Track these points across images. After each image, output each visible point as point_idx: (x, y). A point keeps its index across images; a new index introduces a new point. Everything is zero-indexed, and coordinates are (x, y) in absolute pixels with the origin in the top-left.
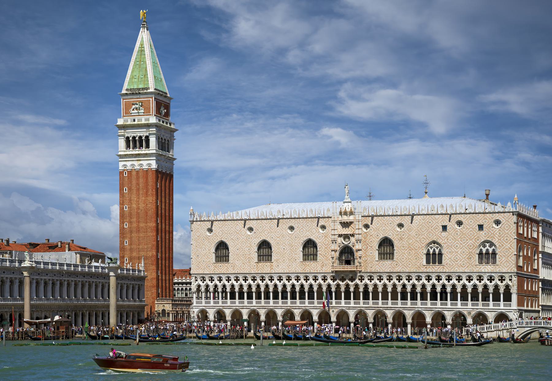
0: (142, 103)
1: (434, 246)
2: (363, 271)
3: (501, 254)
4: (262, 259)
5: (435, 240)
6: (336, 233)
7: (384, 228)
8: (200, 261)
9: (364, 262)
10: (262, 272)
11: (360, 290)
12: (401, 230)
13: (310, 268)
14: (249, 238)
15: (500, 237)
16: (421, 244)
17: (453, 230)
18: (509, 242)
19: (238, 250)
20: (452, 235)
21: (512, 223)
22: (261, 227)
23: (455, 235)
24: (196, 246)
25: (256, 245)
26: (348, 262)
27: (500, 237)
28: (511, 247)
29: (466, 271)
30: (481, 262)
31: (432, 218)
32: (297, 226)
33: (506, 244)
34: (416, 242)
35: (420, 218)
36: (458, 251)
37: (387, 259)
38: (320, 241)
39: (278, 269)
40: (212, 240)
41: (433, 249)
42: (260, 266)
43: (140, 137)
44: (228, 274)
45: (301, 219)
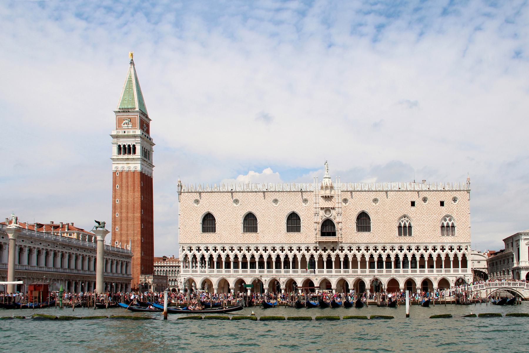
2: (344, 242)
5: (406, 214)
6: (317, 207)
9: (344, 234)
11: (341, 260)
12: (376, 205)
13: (294, 239)
14: (235, 210)
15: (457, 212)
16: (394, 217)
17: (420, 206)
18: (465, 216)
19: (224, 221)
22: (246, 199)
23: (422, 210)
26: (329, 234)
27: (457, 212)
38: (303, 214)
40: (199, 211)
41: (403, 222)
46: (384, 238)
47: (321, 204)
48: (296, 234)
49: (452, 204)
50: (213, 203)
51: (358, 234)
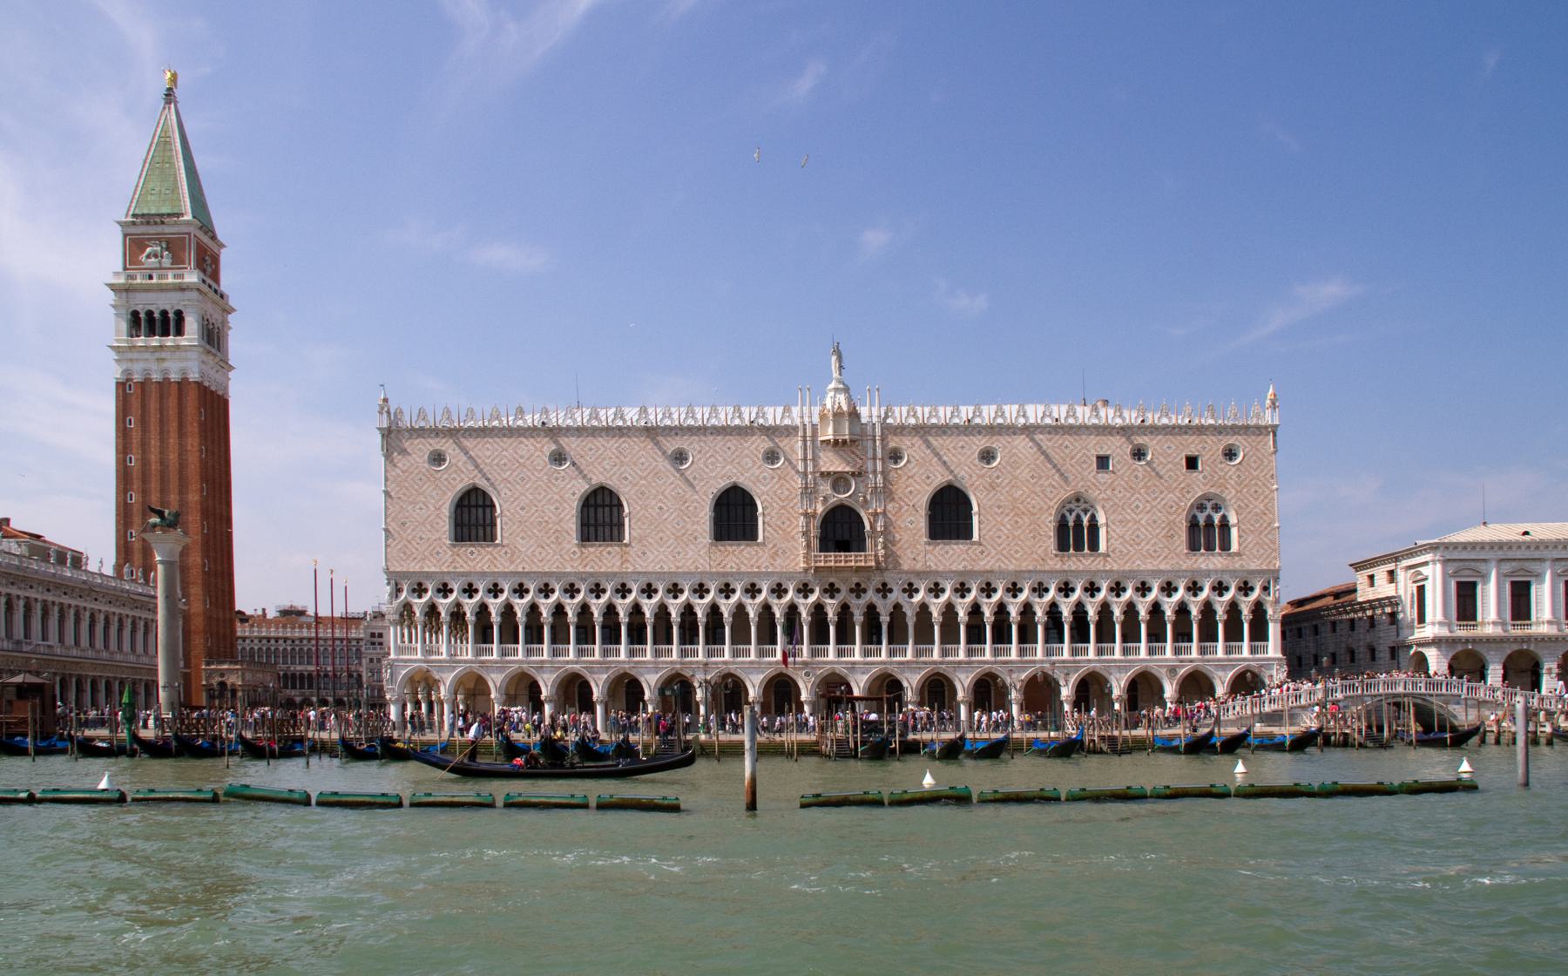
2: (891, 566)
3: (1243, 527)
4: (592, 535)
5: (1083, 490)
8: (409, 538)
10: (597, 569)
14: (557, 479)
18: (1262, 497)
19: (523, 509)
22: (591, 449)
24: (399, 498)
25: (578, 496)
26: (844, 546)
28: (1267, 509)
32: (699, 449)
33: (1254, 502)
34: (1032, 495)
39: (644, 561)
41: (1074, 514)
42: (590, 553)
43: (164, 313)
50: (487, 461)
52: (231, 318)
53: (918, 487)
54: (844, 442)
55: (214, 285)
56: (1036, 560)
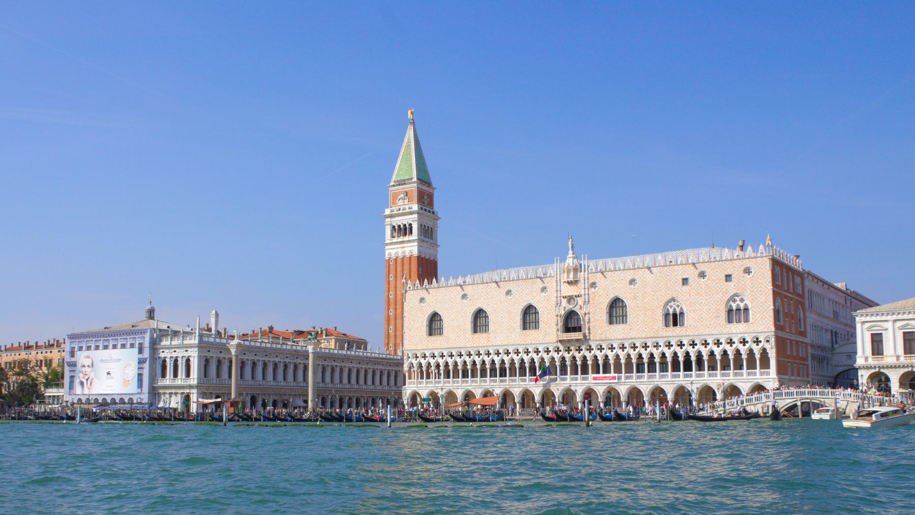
0: (407, 193)
1: (674, 304)
2: (592, 338)
3: (755, 310)
5: (675, 296)
7: (615, 286)
10: (478, 345)
14: (464, 307)
15: (752, 288)
16: (659, 302)
18: (764, 293)
19: (452, 320)
20: (694, 290)
21: (766, 271)
22: (476, 293)
25: (471, 314)
27: (752, 288)
28: (767, 300)
29: (714, 333)
30: (730, 321)
31: (670, 270)
32: (516, 289)
35: (656, 271)
36: (703, 309)
37: (620, 323)
38: (541, 306)
41: (673, 308)
43: (405, 225)
44: (443, 349)
45: (520, 281)
46: (645, 332)
47: (562, 291)
48: (533, 332)
49: (743, 277)
51: (610, 328)
52: (438, 222)
53: (603, 300)
54: (571, 281)
55: (428, 209)
56: (654, 332)
